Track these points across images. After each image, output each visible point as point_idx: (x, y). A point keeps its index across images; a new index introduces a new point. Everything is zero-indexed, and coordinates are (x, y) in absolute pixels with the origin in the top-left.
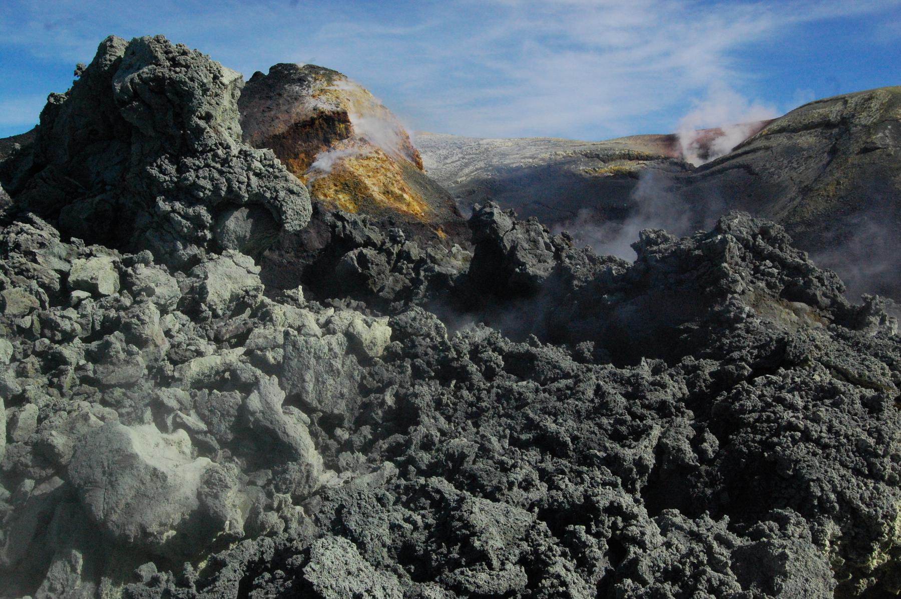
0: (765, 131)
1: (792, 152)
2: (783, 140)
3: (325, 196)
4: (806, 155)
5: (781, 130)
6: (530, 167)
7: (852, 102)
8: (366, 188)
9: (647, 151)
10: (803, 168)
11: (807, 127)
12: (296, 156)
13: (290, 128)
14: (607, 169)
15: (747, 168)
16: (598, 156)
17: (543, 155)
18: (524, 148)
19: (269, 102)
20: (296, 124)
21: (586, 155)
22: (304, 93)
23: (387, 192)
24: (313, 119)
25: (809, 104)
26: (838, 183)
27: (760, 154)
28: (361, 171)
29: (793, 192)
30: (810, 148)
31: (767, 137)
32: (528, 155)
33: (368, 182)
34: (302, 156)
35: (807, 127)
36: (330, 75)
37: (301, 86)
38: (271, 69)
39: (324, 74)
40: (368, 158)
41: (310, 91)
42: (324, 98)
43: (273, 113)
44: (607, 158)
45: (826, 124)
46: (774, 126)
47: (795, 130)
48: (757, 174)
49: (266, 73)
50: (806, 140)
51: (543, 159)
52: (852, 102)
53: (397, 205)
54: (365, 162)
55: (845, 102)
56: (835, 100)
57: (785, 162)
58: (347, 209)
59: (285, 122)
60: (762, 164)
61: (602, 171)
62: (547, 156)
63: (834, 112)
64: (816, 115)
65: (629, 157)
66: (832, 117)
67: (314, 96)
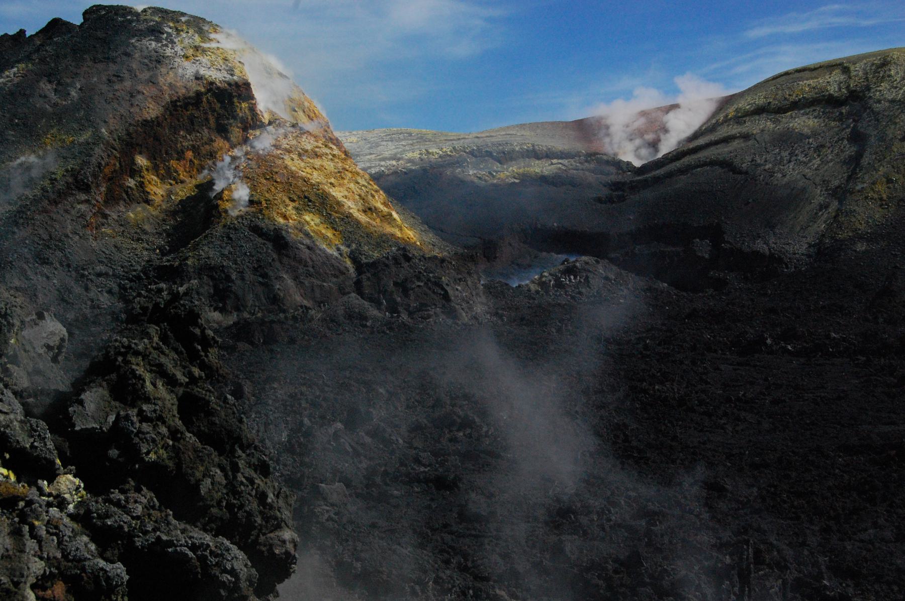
0: (731, 111)
1: (787, 139)
2: (764, 125)
3: (285, 217)
4: (815, 144)
5: (760, 111)
6: (395, 173)
7: (857, 70)
8: (339, 203)
9: (559, 144)
10: (817, 162)
11: (795, 106)
12: (180, 156)
13: (166, 108)
14: (508, 173)
15: (727, 165)
16: (489, 154)
17: (410, 155)
18: (378, 145)
19: (113, 68)
20: (174, 103)
21: (472, 153)
22: (169, 52)
23: (369, 210)
24: (199, 94)
25: (787, 74)
26: (889, 181)
27: (735, 144)
28: (316, 177)
29: (819, 196)
30: (815, 134)
31: (740, 118)
32: (387, 154)
33: (337, 193)
34: (189, 154)
35: (795, 106)
36: (198, 24)
37: (158, 40)
38: (86, 14)
39: (188, 23)
40: (317, 155)
41: (178, 48)
42: (204, 60)
43: (128, 84)
44: (505, 157)
45: (825, 102)
46: (744, 105)
47: (781, 110)
48: (746, 173)
49: (78, 20)
50: (803, 123)
51: (410, 161)
52: (857, 70)
53: (389, 229)
54: (317, 162)
55: (846, 70)
56: (830, 67)
57: (785, 154)
58: (325, 238)
59: (156, 99)
60: (748, 158)
61: (502, 175)
62: (416, 155)
63: (833, 83)
64: (806, 87)
65: (536, 154)
66: (833, 89)
67: (187, 57)
